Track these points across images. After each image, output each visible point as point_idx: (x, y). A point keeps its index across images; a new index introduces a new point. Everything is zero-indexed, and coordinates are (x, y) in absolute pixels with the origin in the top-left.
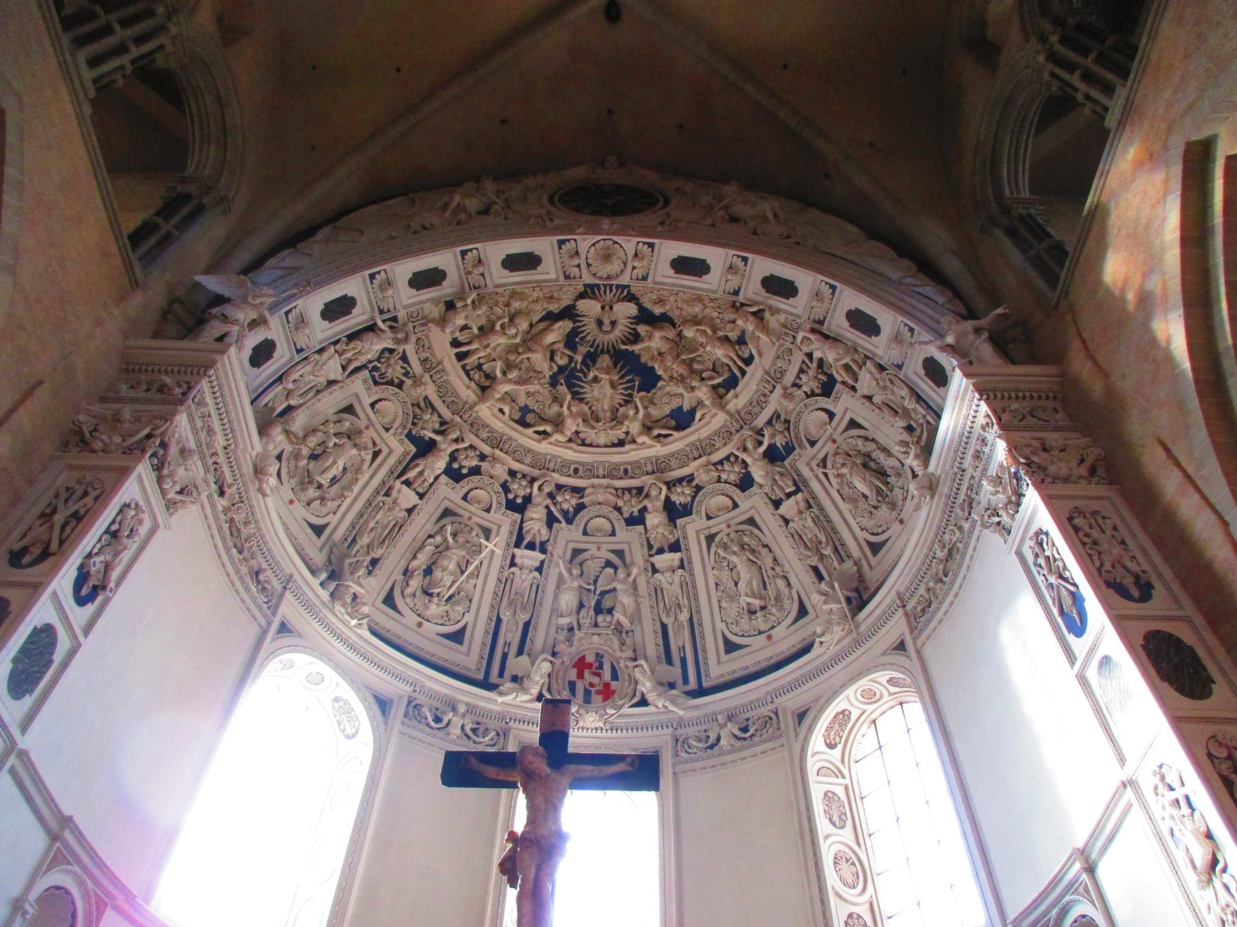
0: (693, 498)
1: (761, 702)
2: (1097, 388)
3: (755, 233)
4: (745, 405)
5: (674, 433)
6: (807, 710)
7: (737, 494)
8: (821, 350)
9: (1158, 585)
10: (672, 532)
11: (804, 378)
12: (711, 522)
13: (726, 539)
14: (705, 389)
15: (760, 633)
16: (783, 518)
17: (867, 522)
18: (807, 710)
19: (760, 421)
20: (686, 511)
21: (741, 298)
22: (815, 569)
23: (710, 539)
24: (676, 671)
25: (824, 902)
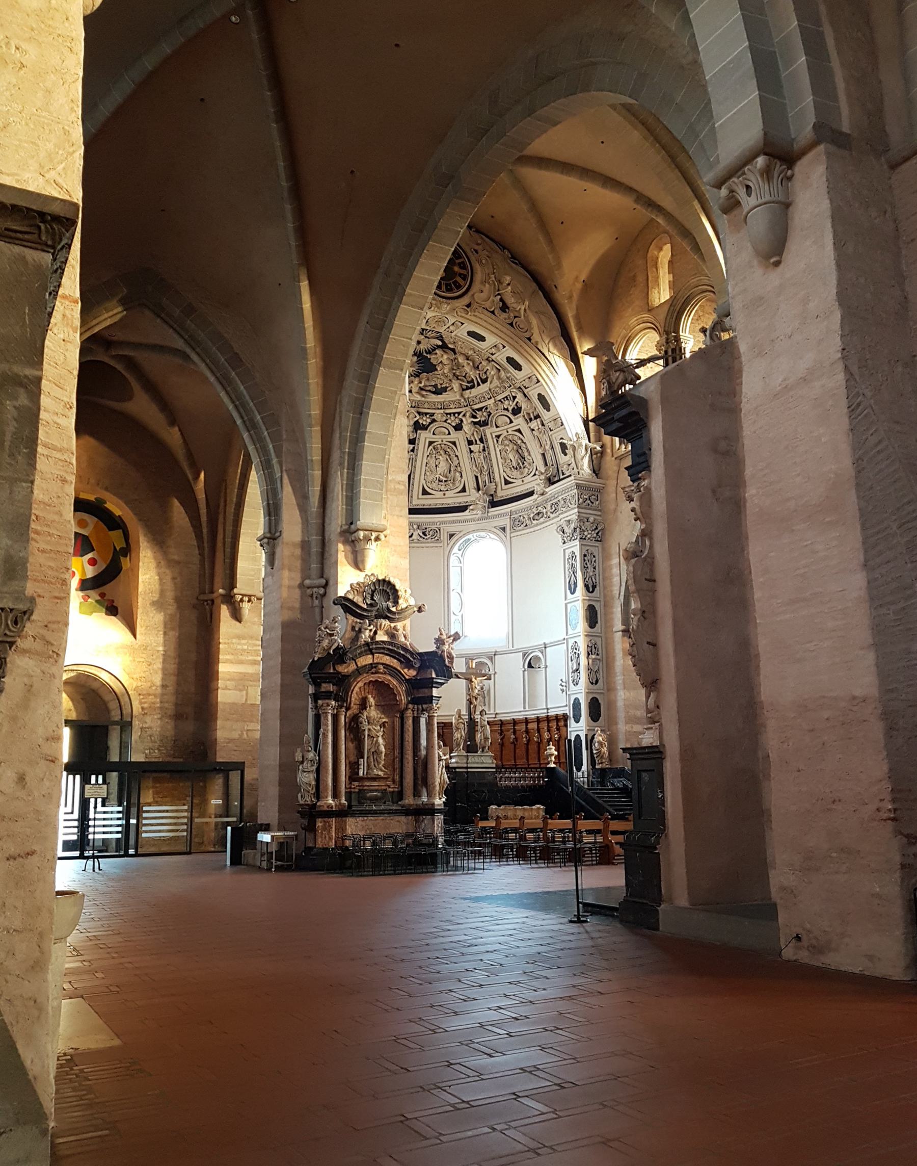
0: (430, 424)
1: (434, 523)
2: (612, 507)
3: (511, 324)
5: (433, 396)
6: (454, 534)
7: (452, 430)
9: (598, 587)
11: (507, 402)
12: (434, 436)
14: (457, 385)
16: (470, 449)
17: (508, 470)
18: (454, 534)
19: (476, 407)
20: (425, 428)
21: (493, 357)
22: (477, 477)
23: (431, 443)
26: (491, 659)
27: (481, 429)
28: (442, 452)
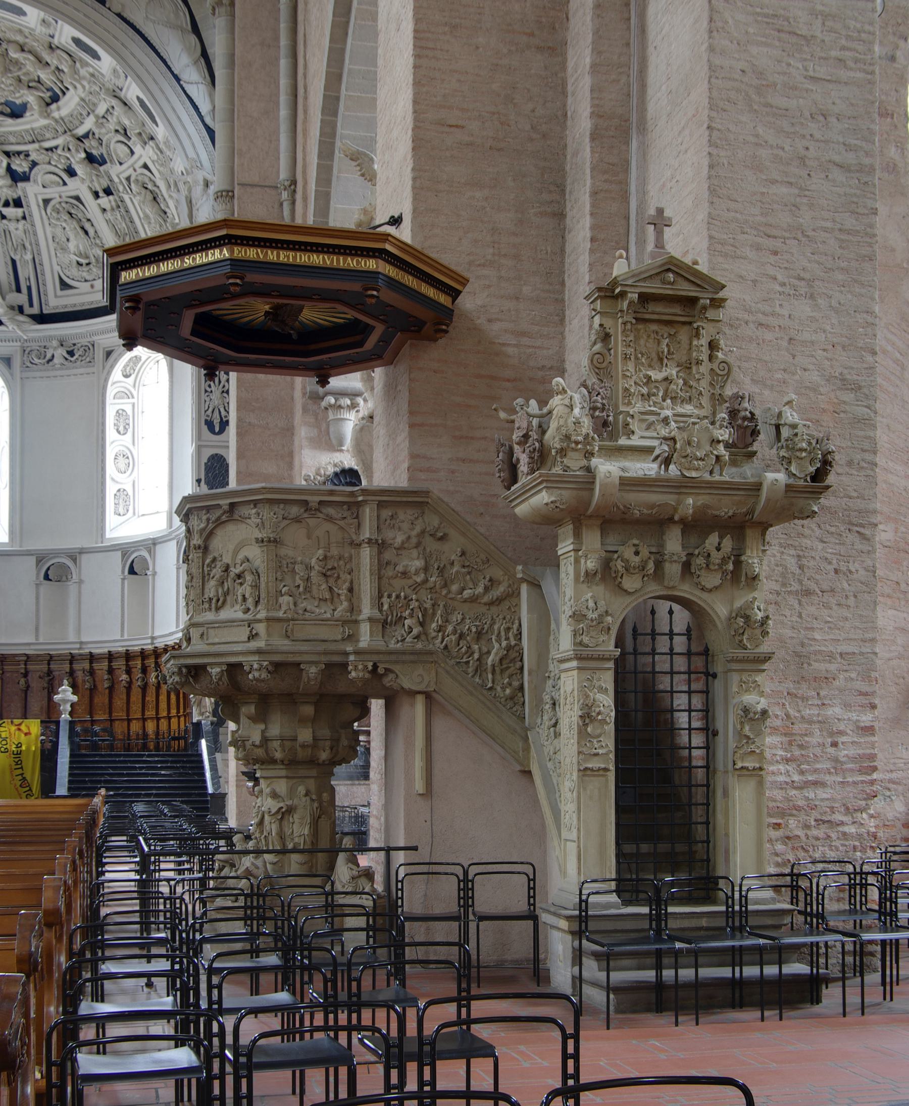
0: (31, 169)
1: (82, 335)
4: (67, 116)
5: (10, 121)
7: (65, 176)
8: (119, 110)
10: (15, 191)
12: (45, 190)
13: (58, 206)
15: (86, 281)
19: (81, 131)
20: (25, 178)
21: (56, 41)
23: (46, 202)
24: (22, 299)
25: (103, 483)
26: (150, 552)
27: (102, 168)
28: (67, 217)
